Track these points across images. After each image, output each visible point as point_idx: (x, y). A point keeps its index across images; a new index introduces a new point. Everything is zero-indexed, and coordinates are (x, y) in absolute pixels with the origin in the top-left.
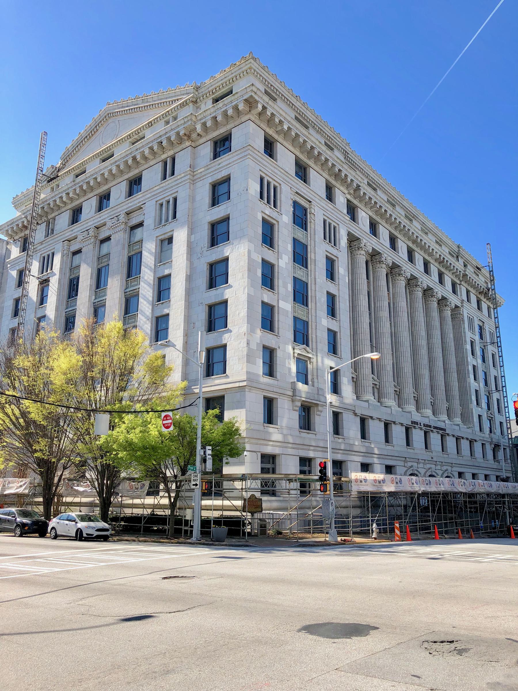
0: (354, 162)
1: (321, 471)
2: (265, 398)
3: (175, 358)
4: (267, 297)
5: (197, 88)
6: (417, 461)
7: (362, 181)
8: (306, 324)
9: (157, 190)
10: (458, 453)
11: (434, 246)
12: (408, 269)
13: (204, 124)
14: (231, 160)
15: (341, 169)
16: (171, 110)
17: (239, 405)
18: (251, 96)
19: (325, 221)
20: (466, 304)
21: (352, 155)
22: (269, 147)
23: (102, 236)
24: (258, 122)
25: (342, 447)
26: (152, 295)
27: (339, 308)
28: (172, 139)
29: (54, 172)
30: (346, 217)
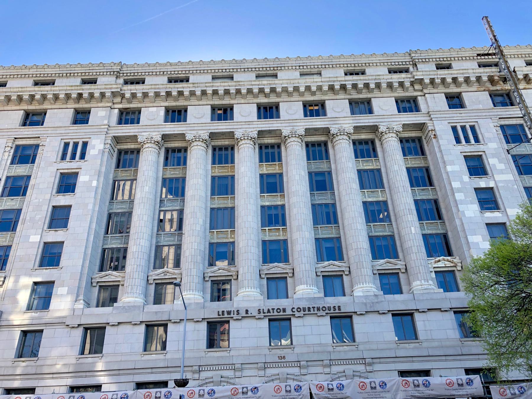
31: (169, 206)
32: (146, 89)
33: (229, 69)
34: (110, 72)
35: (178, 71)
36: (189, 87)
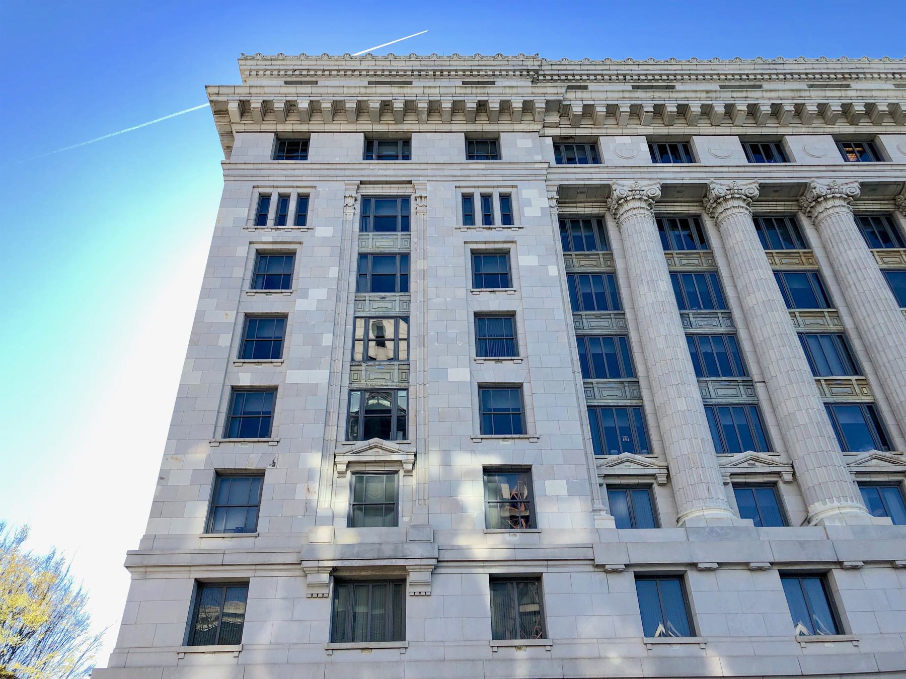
31: (701, 327)
32: (613, 100)
33: (755, 75)
34: (521, 71)
35: (653, 75)
36: (700, 99)
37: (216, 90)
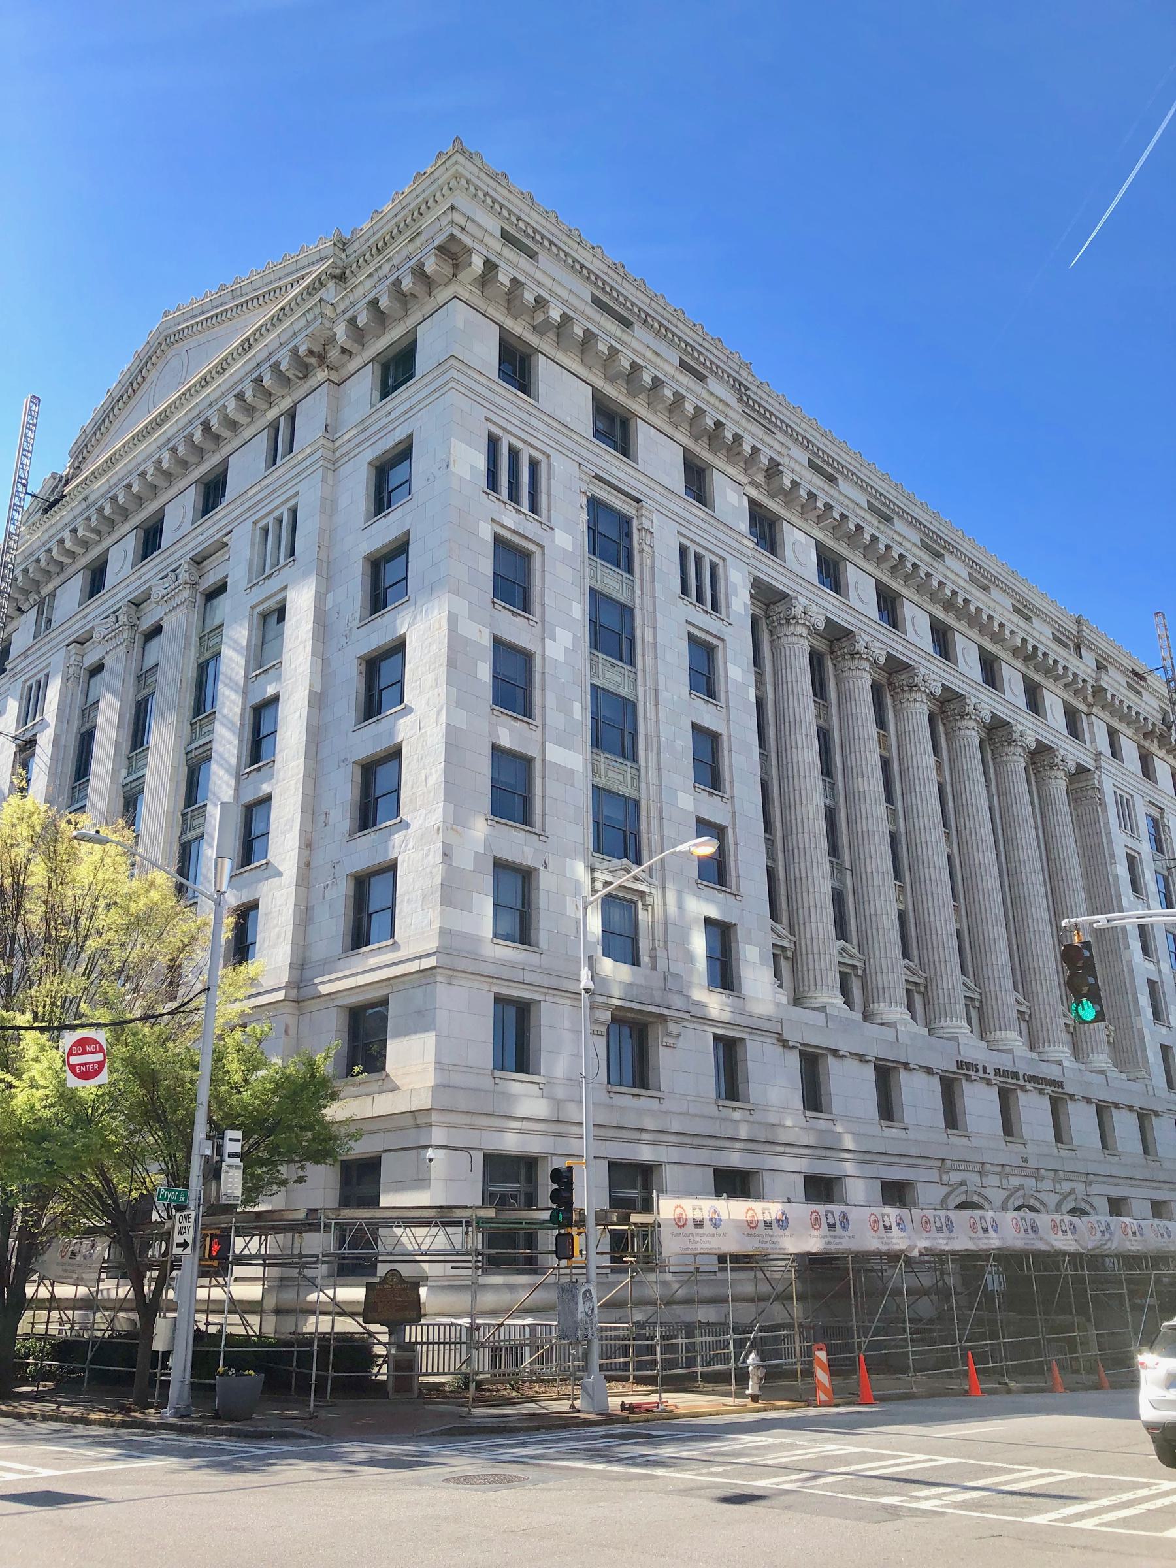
0: (765, 409)
1: (555, 1196)
2: (499, 1000)
3: (278, 902)
4: (510, 733)
5: (343, 245)
6: (978, 1167)
7: (784, 451)
8: (632, 806)
9: (255, 495)
10: (1105, 1145)
11: (1013, 622)
12: (934, 674)
13: (352, 321)
14: (414, 400)
15: (722, 420)
16: (289, 303)
17: (421, 1021)
18: (452, 235)
19: (683, 551)
20: (1108, 763)
21: (759, 392)
22: (517, 367)
23: (146, 624)
24: (481, 304)
25: (743, 1134)
26: (236, 752)
27: (731, 766)
28: (284, 366)
29: (56, 487)
30: (745, 541)
37: (462, 221)
